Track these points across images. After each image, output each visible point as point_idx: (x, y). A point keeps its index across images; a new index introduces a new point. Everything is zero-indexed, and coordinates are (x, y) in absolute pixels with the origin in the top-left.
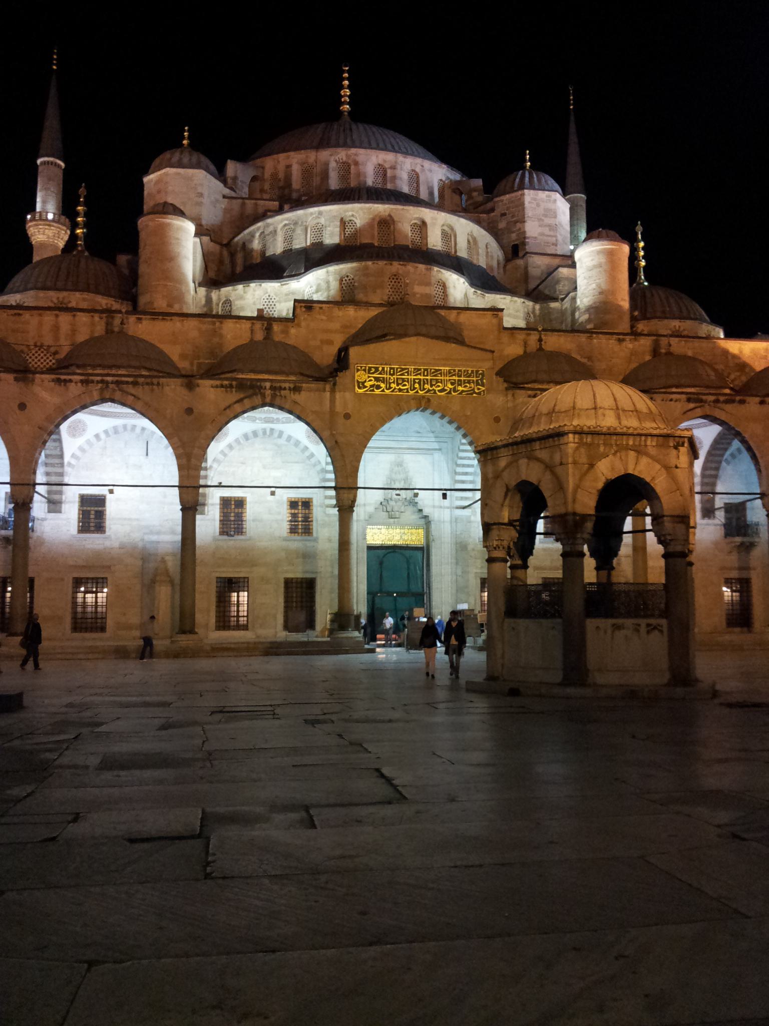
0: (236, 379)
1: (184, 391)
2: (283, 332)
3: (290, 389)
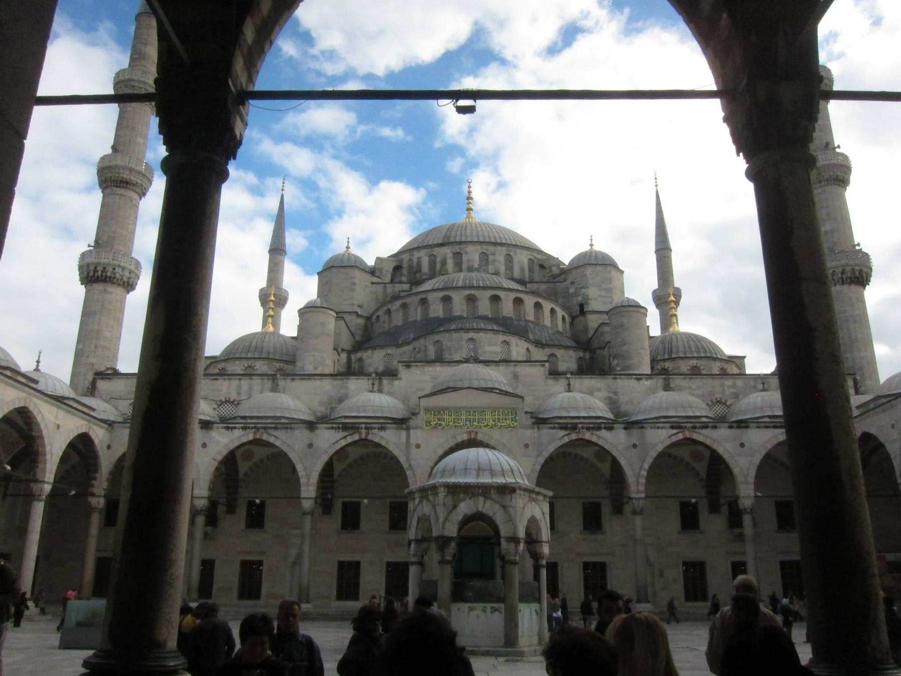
0: (341, 423)
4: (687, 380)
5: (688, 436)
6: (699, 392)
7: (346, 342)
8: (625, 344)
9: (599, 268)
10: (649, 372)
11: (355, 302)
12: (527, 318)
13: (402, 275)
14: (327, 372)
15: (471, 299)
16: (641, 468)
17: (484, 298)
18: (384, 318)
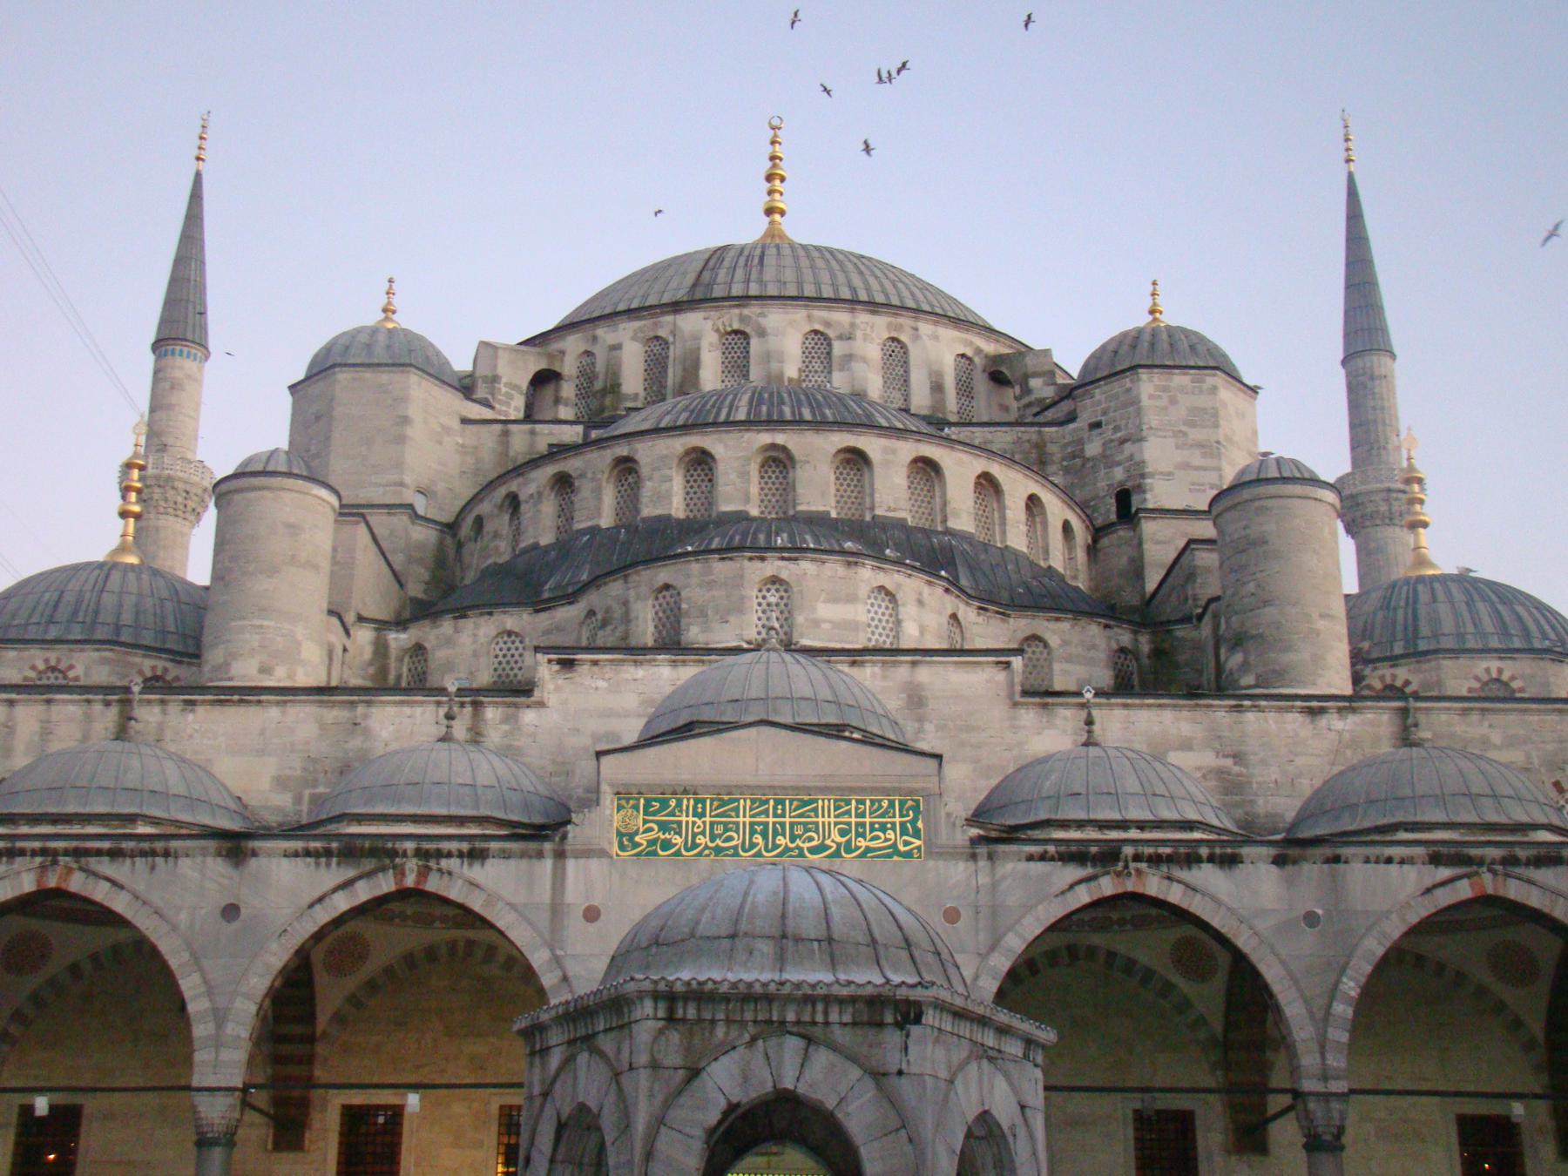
0: (339, 836)
1: (218, 867)
2: (505, 720)
3: (461, 855)
4: (1475, 717)
5: (1490, 891)
6: (1516, 756)
7: (372, 591)
8: (1266, 603)
9: (1180, 379)
10: (1348, 690)
11: (407, 479)
12: (950, 524)
13: (557, 401)
14: (302, 680)
15: (778, 462)
16: (1333, 991)
17: (816, 452)
18: (502, 523)
